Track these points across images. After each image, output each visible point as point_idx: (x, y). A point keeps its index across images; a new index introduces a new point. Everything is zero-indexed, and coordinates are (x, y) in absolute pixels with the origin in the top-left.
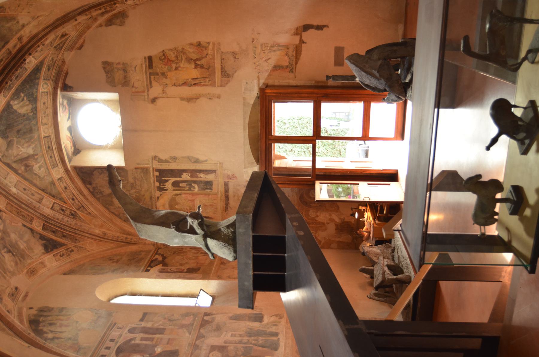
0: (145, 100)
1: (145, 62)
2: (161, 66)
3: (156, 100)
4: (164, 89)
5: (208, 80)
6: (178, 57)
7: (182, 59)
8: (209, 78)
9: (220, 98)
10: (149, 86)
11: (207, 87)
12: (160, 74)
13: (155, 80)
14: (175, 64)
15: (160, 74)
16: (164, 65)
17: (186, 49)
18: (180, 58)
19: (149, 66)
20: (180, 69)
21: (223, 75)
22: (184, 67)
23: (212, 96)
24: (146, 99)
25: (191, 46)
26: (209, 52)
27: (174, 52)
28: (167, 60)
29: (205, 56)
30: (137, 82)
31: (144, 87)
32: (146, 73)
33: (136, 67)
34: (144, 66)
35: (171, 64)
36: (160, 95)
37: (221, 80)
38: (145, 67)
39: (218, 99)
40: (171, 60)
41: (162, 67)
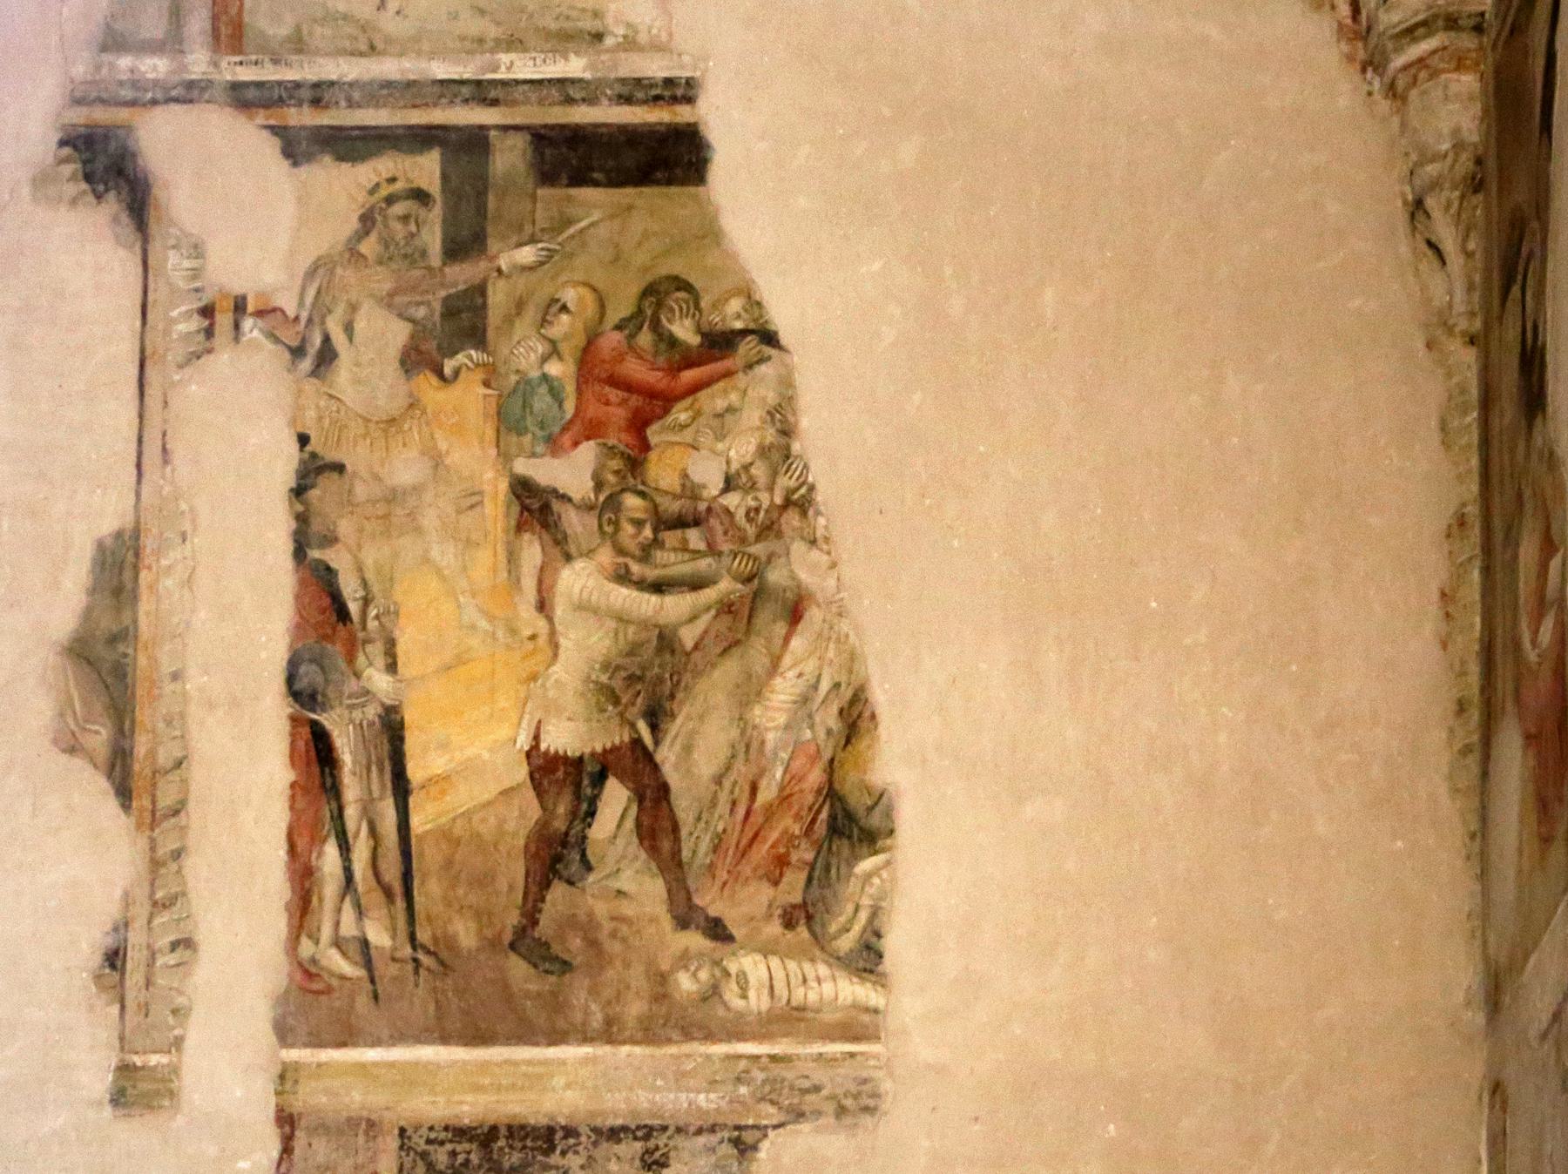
0: (113, 41)
1: (633, 91)
2: (570, 296)
3: (112, 205)
4: (260, 314)
6: (694, 537)
7: (658, 587)
8: (408, 951)
9: (119, 1098)
10: (301, 117)
11: (279, 924)
12: (462, 274)
13: (390, 200)
14: (599, 485)
15: (462, 274)
16: (580, 340)
17: (796, 643)
18: (670, 563)
19: (576, 137)
20: (532, 552)
22: (560, 611)
23: (149, 983)
24: (125, 62)
25: (829, 718)
26: (752, 965)
27: (753, 486)
29: (697, 901)
31: (298, 45)
32: (482, 92)
34: (574, 66)
35: (592, 430)
36: (174, 264)
38: (561, 82)
39: (98, 1081)
40: (654, 434)
41: (564, 308)
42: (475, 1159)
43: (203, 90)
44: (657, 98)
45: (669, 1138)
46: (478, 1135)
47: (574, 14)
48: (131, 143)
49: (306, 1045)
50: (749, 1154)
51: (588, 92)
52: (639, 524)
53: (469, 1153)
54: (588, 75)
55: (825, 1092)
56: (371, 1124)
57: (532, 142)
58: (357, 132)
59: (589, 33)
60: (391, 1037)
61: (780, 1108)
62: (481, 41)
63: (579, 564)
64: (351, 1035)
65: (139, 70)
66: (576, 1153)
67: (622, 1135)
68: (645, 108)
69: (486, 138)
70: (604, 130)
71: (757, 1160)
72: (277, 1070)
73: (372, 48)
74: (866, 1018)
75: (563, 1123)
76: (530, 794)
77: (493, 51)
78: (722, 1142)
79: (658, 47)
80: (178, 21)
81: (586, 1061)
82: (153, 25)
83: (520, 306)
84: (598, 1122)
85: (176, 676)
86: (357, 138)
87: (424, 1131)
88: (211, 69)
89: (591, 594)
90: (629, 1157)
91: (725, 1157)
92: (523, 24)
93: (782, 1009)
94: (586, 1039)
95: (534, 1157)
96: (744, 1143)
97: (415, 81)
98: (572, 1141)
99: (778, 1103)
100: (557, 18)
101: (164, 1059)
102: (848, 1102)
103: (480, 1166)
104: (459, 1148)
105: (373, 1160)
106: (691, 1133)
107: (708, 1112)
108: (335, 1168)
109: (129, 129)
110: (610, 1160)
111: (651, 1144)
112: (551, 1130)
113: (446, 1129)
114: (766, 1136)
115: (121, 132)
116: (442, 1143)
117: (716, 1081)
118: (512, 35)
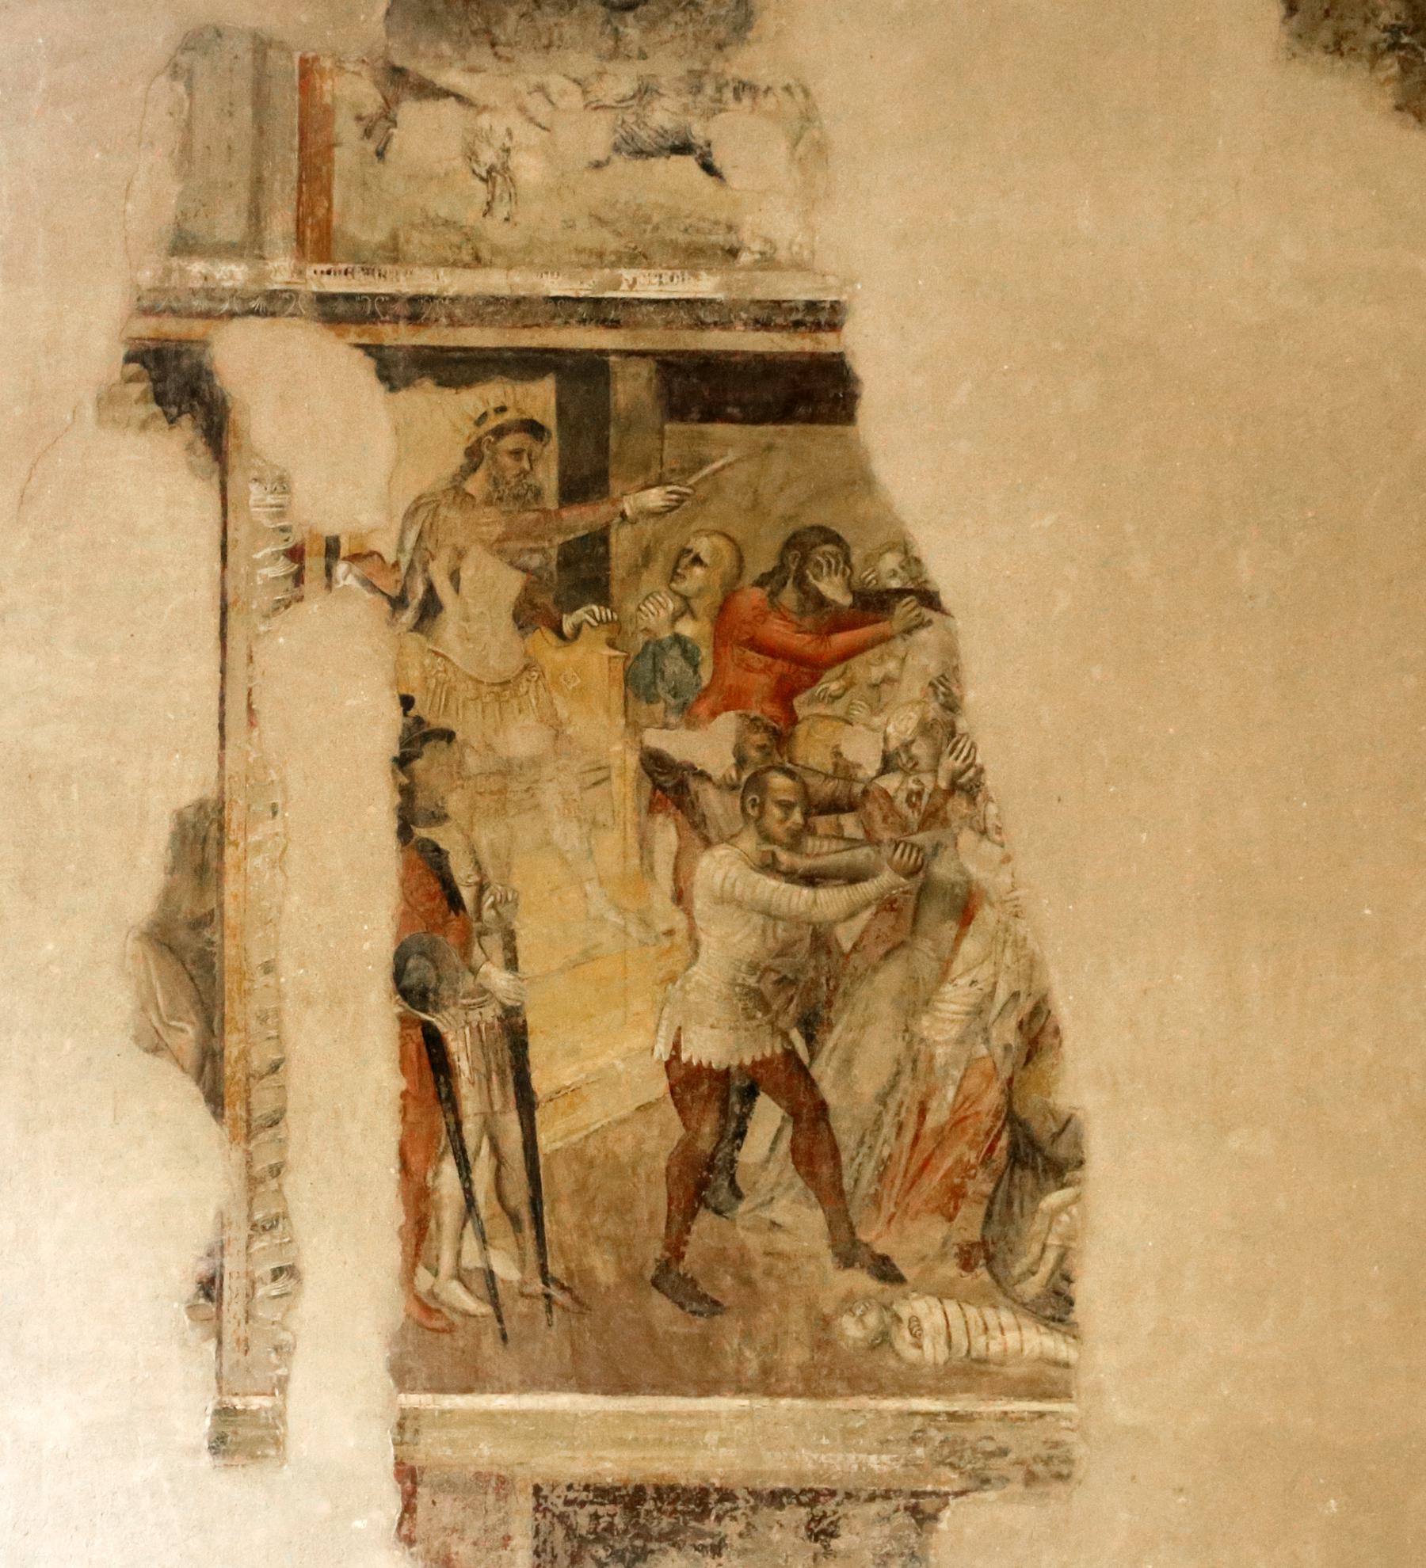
0: (183, 245)
2: (703, 546)
3: (187, 430)
4: (354, 558)
5: (505, 1268)
6: (850, 824)
7: (811, 879)
8: (538, 1286)
9: (219, 1445)
10: (399, 336)
11: (391, 1252)
12: (582, 518)
13: (500, 432)
14: (741, 762)
15: (582, 518)
16: (714, 597)
17: (970, 947)
18: (822, 852)
19: (708, 365)
20: (666, 835)
21: (582, 1520)
22: (699, 905)
23: (248, 1316)
24: (197, 267)
25: (1006, 1033)
26: (924, 1309)
28: (802, 643)
29: (863, 1236)
30: (471, 155)
31: (394, 253)
33: (688, 165)
34: (705, 285)
35: (732, 700)
36: (257, 498)
37: (503, 1484)
41: (697, 560)
42: (619, 1523)
43: (287, 301)
44: (797, 324)
45: (838, 1505)
46: (622, 1497)
47: (705, 225)
48: (205, 360)
49: (426, 1390)
50: (927, 1525)
51: (720, 314)
52: (787, 807)
53: (613, 1516)
54: (720, 296)
55: (1012, 1456)
56: (502, 1481)
57: (657, 371)
58: (458, 355)
59: (722, 249)
60: (523, 1382)
61: (961, 1473)
62: (601, 255)
63: (720, 851)
64: (477, 1378)
65: (213, 277)
66: (734, 1519)
67: (785, 1500)
68: (785, 334)
69: (606, 364)
70: (738, 358)
71: (937, 1531)
72: (394, 1420)
73: (477, 258)
74: (1054, 1373)
75: (718, 1485)
76: (672, 1111)
77: (613, 265)
78: (897, 1510)
79: (799, 266)
80: (258, 221)
81: (739, 1416)
82: (230, 225)
83: (647, 556)
84: (757, 1485)
85: (268, 968)
86: (461, 361)
87: (561, 1490)
88: (295, 279)
89: (733, 886)
90: (794, 1524)
91: (900, 1527)
92: (648, 235)
93: (961, 1360)
94: (741, 1390)
95: (686, 1523)
96: (922, 1512)
97: (524, 298)
98: (728, 1505)
99: (959, 1468)
100: (686, 230)
101: (265, 1402)
102: (1039, 1468)
103: (626, 1531)
104: (601, 1511)
105: (504, 1521)
106: (862, 1498)
107: (880, 1477)
108: (463, 1531)
109: (205, 344)
110: (771, 1528)
111: (818, 1510)
112: (704, 1493)
113: (587, 1488)
114: (947, 1504)
115: (196, 348)
116: (583, 1504)
117: (888, 1441)
118: (636, 248)
